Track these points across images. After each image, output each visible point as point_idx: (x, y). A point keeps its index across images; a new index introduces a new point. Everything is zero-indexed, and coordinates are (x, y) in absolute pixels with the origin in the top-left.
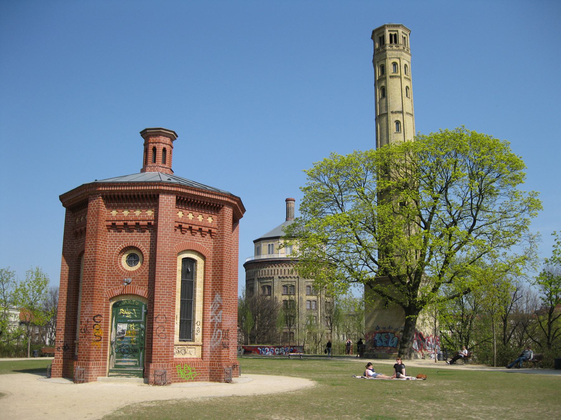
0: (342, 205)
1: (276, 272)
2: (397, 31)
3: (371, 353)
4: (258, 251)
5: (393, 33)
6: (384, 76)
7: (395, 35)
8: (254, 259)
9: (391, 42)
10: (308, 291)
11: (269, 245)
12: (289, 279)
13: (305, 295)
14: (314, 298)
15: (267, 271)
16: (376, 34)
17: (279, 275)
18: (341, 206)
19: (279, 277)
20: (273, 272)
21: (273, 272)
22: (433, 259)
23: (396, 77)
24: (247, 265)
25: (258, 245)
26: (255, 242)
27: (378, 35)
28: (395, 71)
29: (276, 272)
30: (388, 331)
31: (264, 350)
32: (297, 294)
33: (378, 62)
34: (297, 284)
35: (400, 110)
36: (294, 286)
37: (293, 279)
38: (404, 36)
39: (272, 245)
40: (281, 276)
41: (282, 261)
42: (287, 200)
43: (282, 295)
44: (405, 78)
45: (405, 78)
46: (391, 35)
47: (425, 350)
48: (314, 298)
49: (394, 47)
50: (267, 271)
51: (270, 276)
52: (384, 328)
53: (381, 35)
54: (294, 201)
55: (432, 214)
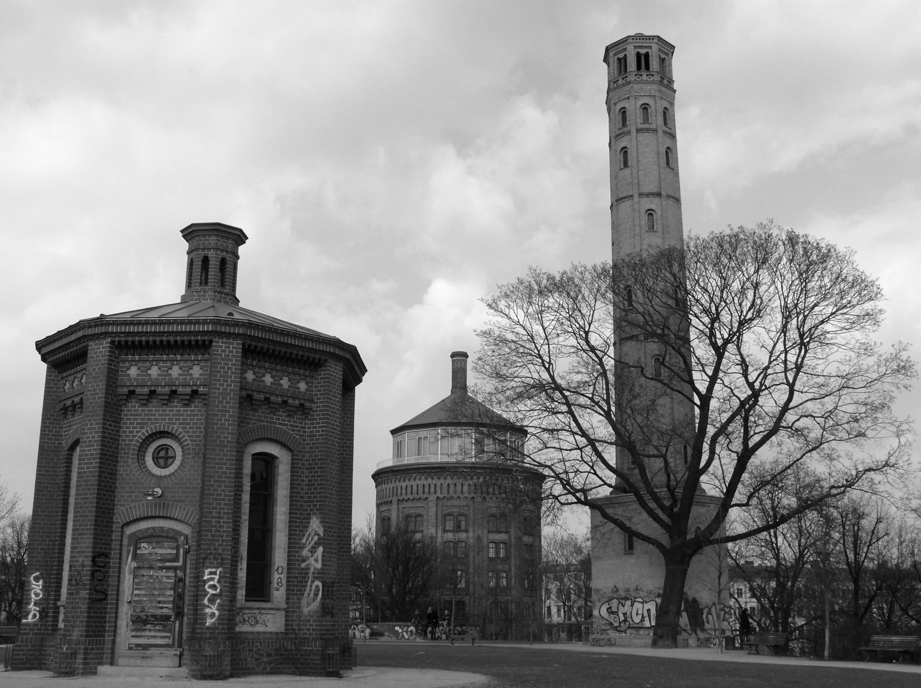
0: (550, 363)
1: (432, 490)
2: (650, 47)
3: (603, 636)
4: (398, 449)
5: (643, 51)
6: (626, 129)
7: (647, 55)
8: (390, 464)
9: (639, 68)
11: (420, 439)
13: (486, 531)
14: (503, 537)
15: (415, 488)
16: (611, 54)
17: (438, 494)
18: (547, 365)
20: (427, 490)
21: (427, 490)
22: (716, 462)
23: (648, 130)
24: (380, 476)
25: (399, 439)
26: (394, 432)
27: (615, 55)
28: (646, 120)
29: (432, 490)
30: (633, 594)
31: (407, 632)
32: (471, 529)
33: (615, 104)
35: (655, 190)
38: (663, 56)
39: (426, 438)
40: (441, 496)
41: (445, 468)
42: (454, 355)
43: (445, 531)
44: (665, 132)
45: (665, 132)
46: (638, 55)
47: (703, 630)
48: (503, 537)
49: (644, 77)
50: (415, 488)
51: (421, 495)
52: (628, 590)
53: (621, 56)
55: (713, 379)
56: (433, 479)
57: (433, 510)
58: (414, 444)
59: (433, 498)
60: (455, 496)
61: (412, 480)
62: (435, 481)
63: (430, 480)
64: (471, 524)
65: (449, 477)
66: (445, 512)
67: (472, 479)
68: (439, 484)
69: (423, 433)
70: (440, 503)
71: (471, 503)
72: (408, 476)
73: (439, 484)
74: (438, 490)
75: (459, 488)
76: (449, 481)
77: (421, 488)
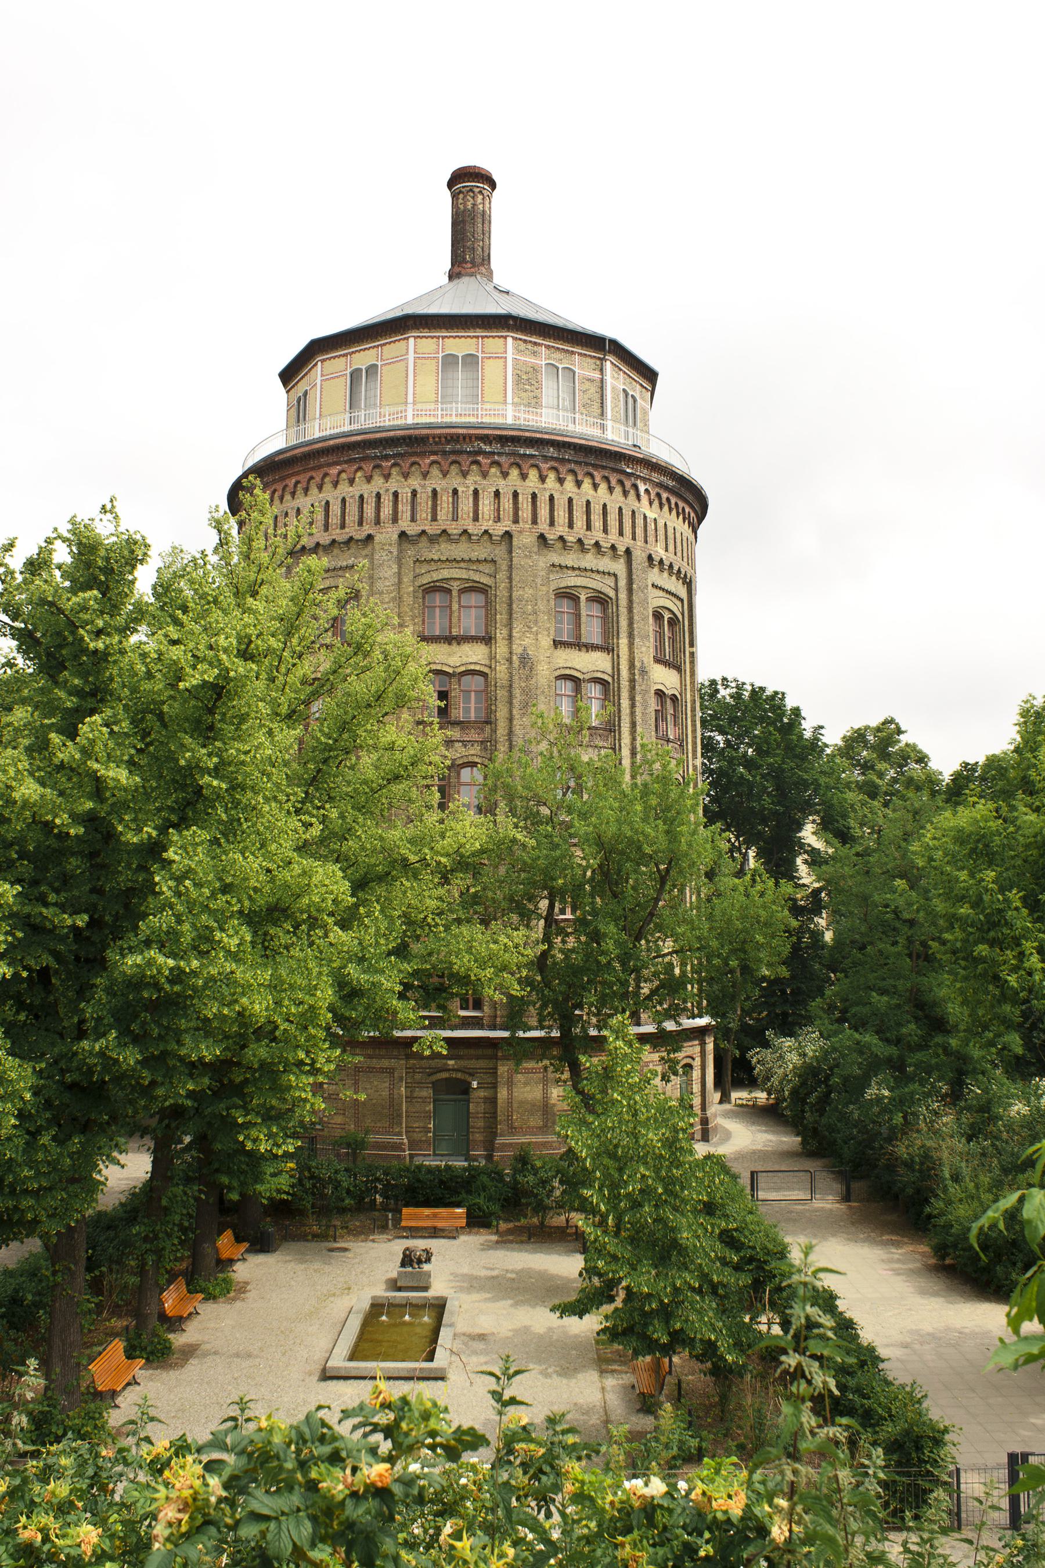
1: (386, 510)
10: (567, 627)
11: (355, 375)
12: (461, 550)
15: (335, 509)
17: (405, 524)
19: (403, 535)
20: (369, 510)
21: (369, 510)
26: (289, 375)
29: (386, 510)
34: (502, 576)
36: (482, 589)
37: (481, 552)
39: (372, 369)
40: (412, 530)
48: (596, 663)
50: (335, 509)
51: (352, 530)
54: (493, 185)
56: (387, 477)
57: (388, 572)
58: (340, 388)
59: (387, 535)
60: (454, 529)
61: (328, 486)
62: (395, 483)
63: (378, 482)
64: (501, 618)
65: (435, 471)
66: (425, 579)
67: (505, 475)
68: (405, 494)
69: (363, 357)
70: (411, 552)
71: (499, 552)
72: (318, 476)
73: (405, 494)
74: (405, 509)
75: (466, 505)
76: (436, 481)
77: (352, 509)
